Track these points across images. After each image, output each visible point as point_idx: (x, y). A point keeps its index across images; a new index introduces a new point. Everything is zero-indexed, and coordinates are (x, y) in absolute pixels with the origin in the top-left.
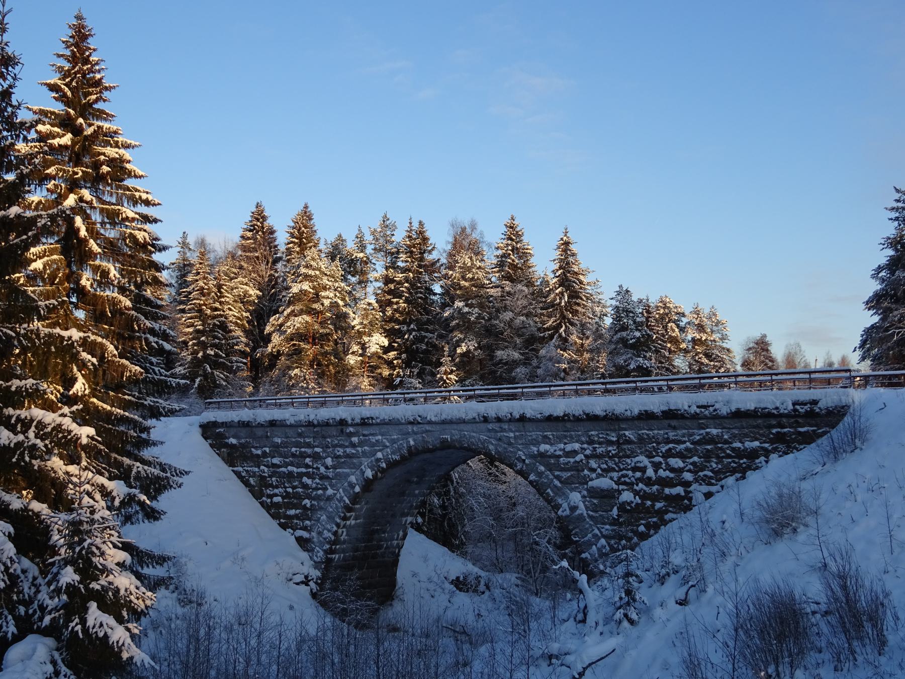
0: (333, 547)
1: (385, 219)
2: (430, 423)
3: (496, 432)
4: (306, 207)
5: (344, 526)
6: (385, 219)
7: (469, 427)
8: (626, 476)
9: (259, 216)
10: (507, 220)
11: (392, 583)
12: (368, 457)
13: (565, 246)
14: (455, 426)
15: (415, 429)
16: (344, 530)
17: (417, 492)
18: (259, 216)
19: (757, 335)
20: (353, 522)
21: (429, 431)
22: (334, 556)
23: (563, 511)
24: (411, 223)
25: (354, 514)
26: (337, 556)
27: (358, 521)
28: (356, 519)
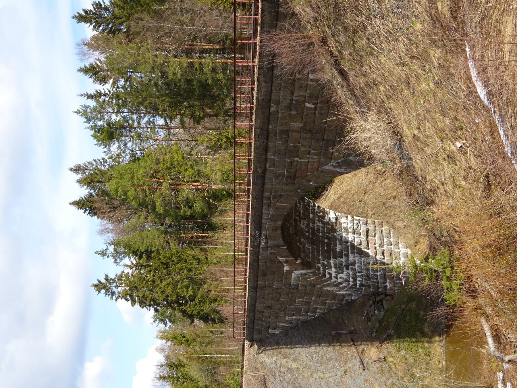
0: (351, 283)
1: (78, 112)
4: (71, 169)
5: (336, 277)
6: (78, 112)
7: (264, 216)
9: (80, 204)
10: (75, 21)
16: (339, 276)
17: (311, 216)
18: (80, 204)
20: (333, 270)
21: (266, 238)
22: (358, 282)
24: (82, 95)
25: (327, 271)
26: (358, 279)
27: (332, 265)
28: (330, 268)
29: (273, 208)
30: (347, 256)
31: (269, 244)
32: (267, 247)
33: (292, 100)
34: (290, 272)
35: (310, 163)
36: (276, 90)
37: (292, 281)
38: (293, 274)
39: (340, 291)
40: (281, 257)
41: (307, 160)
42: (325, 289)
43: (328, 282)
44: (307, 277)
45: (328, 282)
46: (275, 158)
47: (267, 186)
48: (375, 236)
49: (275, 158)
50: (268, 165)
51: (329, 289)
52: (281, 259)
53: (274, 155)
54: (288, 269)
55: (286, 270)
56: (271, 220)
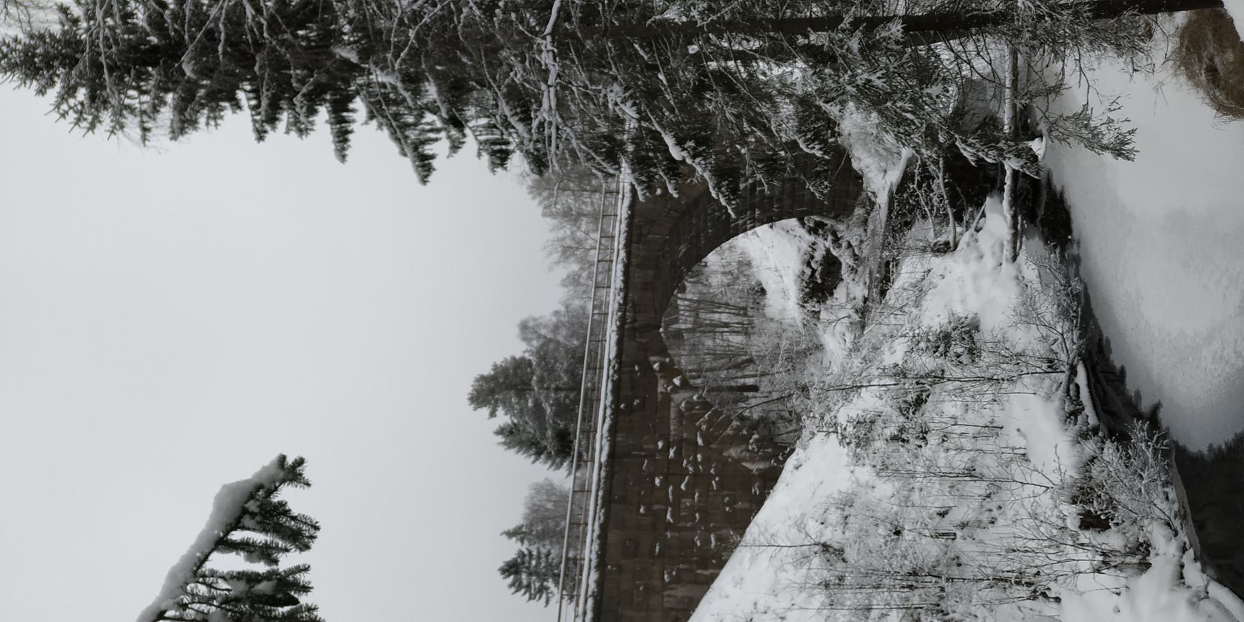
2: (625, 298)
3: (641, 235)
12: (657, 384)
21: (634, 303)
31: (636, 325)
34: (667, 398)
37: (672, 433)
38: (672, 404)
39: (752, 460)
40: (653, 355)
42: (725, 454)
43: (729, 431)
44: (694, 412)
45: (729, 431)
51: (733, 452)
52: (653, 359)
54: (663, 390)
55: (662, 393)
56: (638, 266)
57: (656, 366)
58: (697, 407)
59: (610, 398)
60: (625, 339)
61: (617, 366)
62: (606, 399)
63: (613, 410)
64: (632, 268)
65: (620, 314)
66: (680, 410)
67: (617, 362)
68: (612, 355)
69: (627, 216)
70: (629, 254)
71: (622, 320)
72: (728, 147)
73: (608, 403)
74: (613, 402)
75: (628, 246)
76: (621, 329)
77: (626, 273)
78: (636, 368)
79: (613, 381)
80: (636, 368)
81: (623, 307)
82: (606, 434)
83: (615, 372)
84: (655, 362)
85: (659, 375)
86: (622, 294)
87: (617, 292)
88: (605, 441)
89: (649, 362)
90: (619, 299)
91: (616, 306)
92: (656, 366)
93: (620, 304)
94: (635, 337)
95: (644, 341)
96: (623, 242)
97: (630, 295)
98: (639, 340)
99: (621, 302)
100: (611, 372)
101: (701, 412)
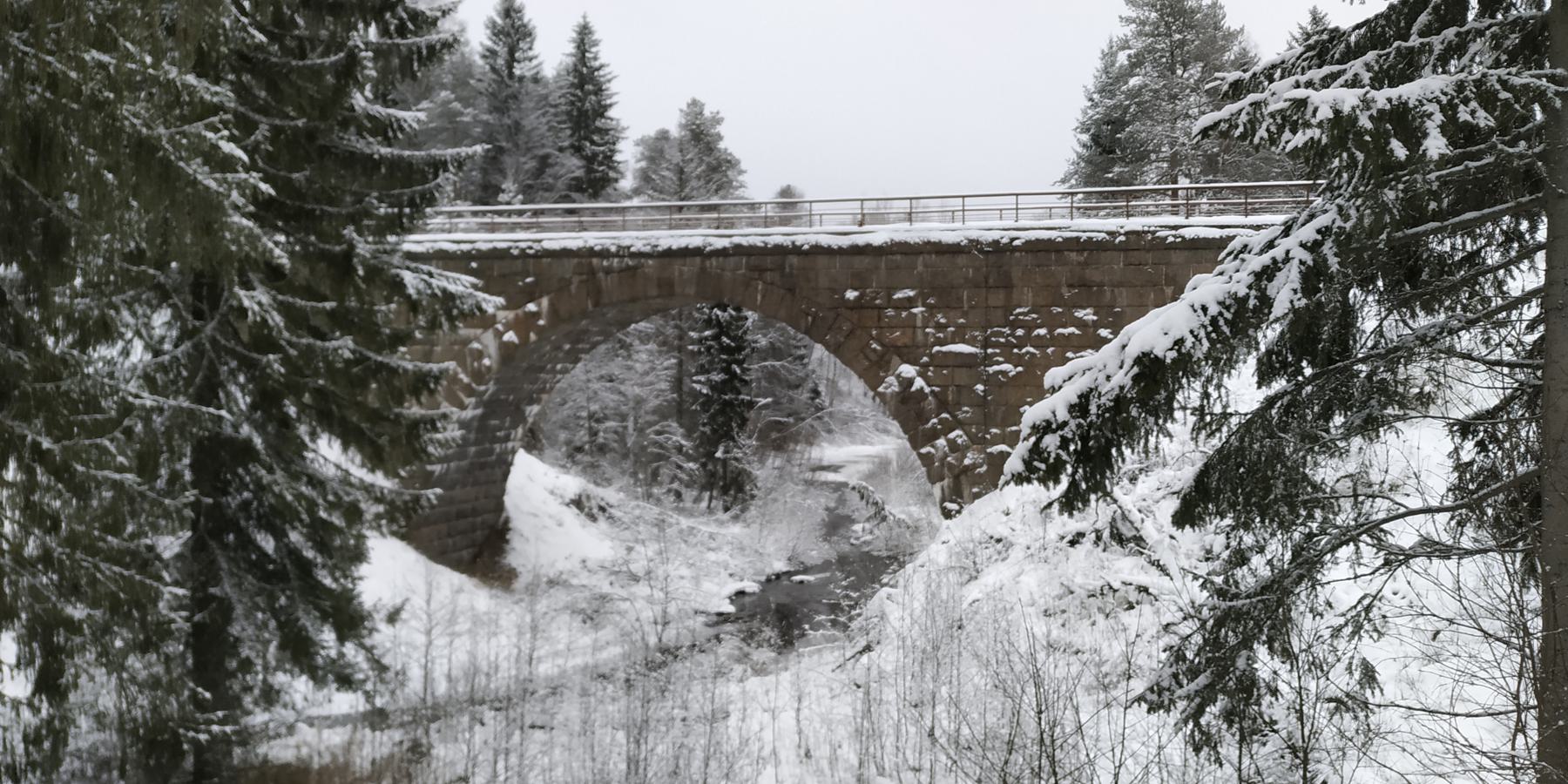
2: (640, 255)
3: (761, 270)
8: (1001, 334)
11: (500, 507)
13: (584, 38)
14: (688, 260)
15: (605, 263)
17: (559, 367)
19: (785, 185)
21: (635, 268)
23: (886, 388)
29: (744, 275)
30: (476, 443)
31: (601, 275)
32: (592, 272)
33: (1101, 285)
35: (909, 331)
36: (1126, 257)
38: (479, 331)
41: (919, 323)
44: (469, 360)
46: (920, 268)
47: (822, 261)
48: (486, 497)
49: (920, 268)
50: (899, 257)
52: (545, 302)
53: (926, 266)
57: (531, 307)
58: (476, 364)
59: (484, 247)
60: (576, 261)
61: (531, 252)
62: (485, 241)
63: (469, 252)
64: (698, 260)
65: (613, 249)
66: (471, 341)
67: (537, 251)
68: (547, 245)
69: (798, 243)
70: (722, 253)
71: (604, 254)
72: (954, 417)
73: (477, 246)
74: (479, 251)
75: (738, 250)
76: (590, 252)
77: (686, 253)
78: (529, 280)
79: (510, 248)
80: (529, 280)
81: (624, 252)
82: (438, 246)
83: (523, 250)
84: (539, 305)
85: (520, 312)
86: (648, 249)
87: (654, 242)
88: (428, 245)
89: (541, 297)
90: (638, 246)
91: (626, 243)
92: (531, 307)
93: (629, 248)
94: (581, 274)
95: (573, 288)
96: (744, 241)
97: (650, 262)
98: (576, 280)
99: (632, 249)
100: (523, 245)
101: (469, 369)
